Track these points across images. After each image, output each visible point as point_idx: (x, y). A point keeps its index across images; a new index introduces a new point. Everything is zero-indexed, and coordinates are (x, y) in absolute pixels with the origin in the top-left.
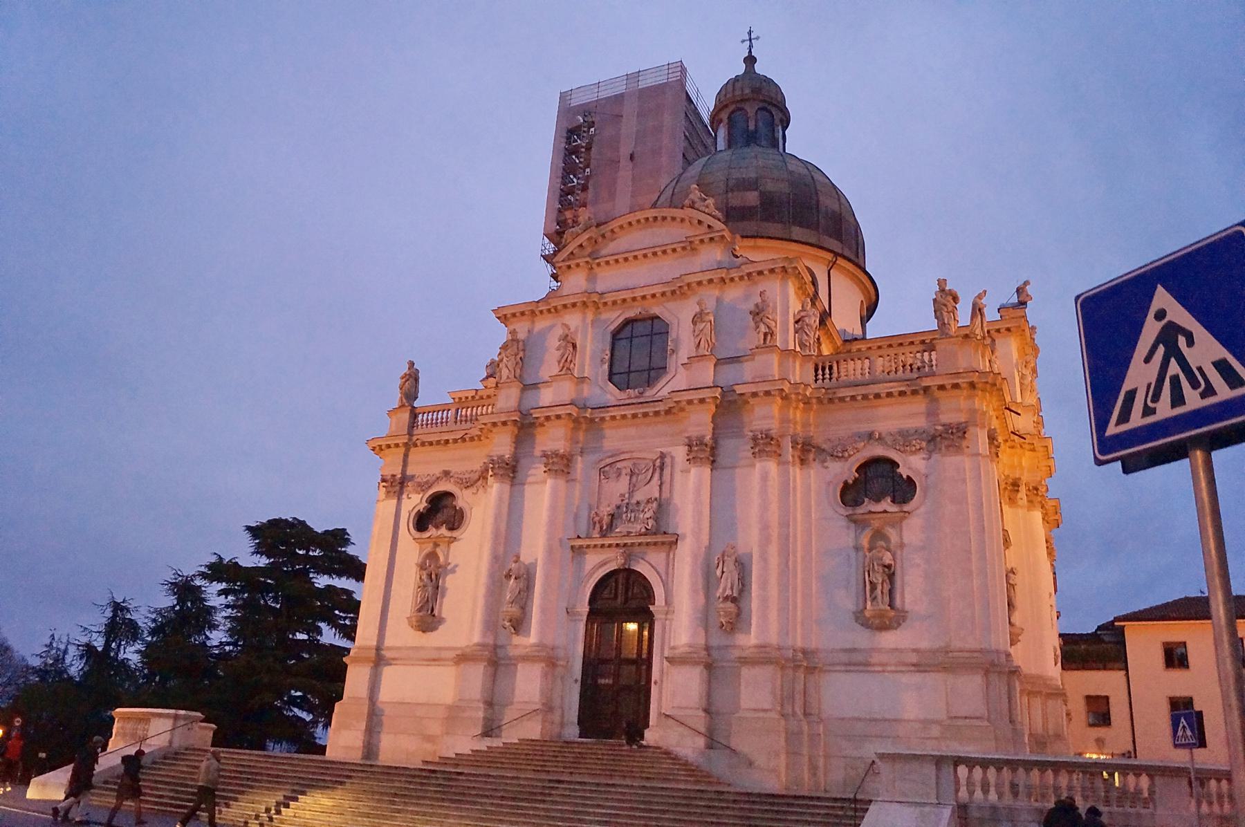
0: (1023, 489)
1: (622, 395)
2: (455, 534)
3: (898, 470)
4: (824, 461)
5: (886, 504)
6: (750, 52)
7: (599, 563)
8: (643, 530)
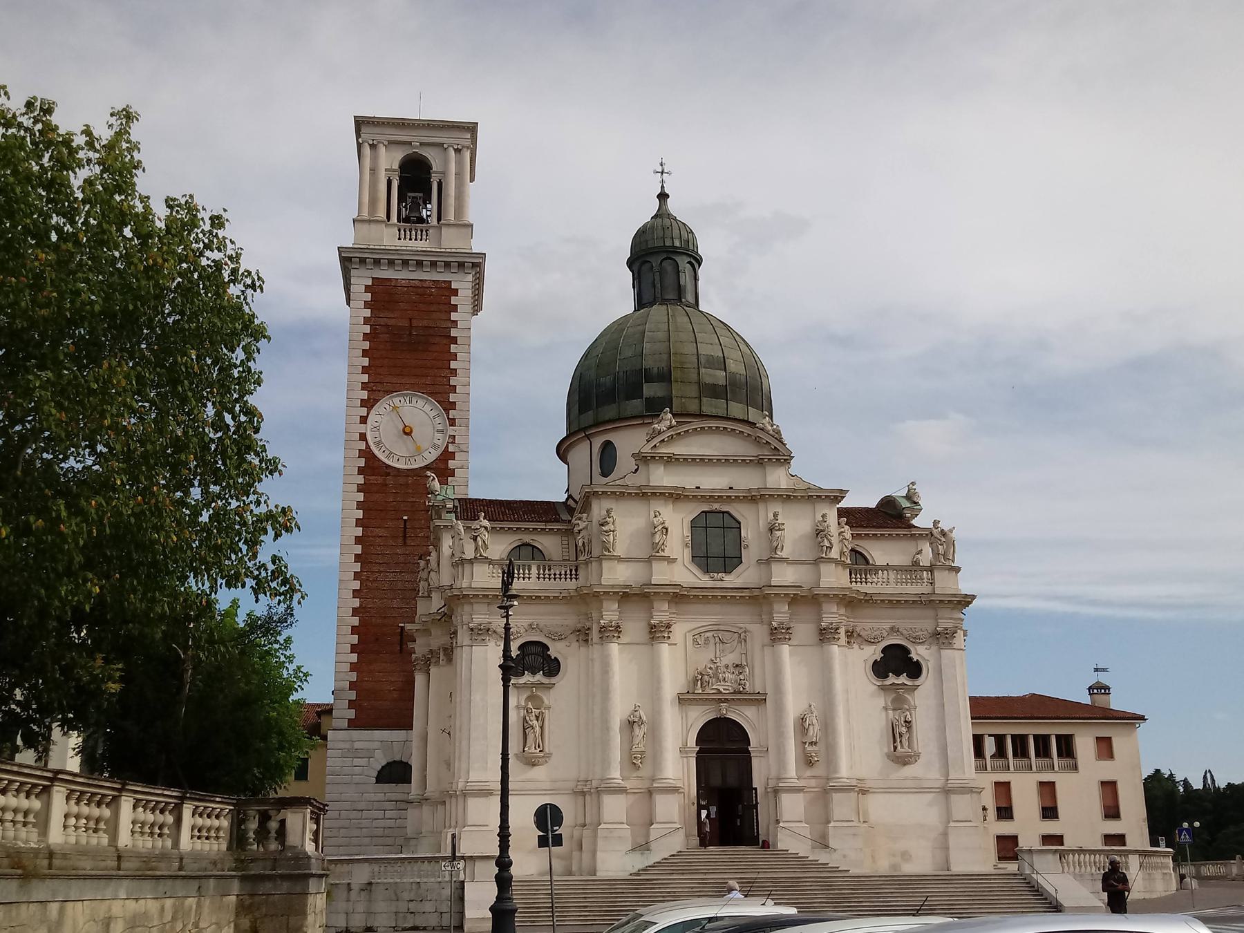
1: (706, 577)
2: (553, 680)
5: (903, 679)
6: (662, 187)
8: (741, 689)
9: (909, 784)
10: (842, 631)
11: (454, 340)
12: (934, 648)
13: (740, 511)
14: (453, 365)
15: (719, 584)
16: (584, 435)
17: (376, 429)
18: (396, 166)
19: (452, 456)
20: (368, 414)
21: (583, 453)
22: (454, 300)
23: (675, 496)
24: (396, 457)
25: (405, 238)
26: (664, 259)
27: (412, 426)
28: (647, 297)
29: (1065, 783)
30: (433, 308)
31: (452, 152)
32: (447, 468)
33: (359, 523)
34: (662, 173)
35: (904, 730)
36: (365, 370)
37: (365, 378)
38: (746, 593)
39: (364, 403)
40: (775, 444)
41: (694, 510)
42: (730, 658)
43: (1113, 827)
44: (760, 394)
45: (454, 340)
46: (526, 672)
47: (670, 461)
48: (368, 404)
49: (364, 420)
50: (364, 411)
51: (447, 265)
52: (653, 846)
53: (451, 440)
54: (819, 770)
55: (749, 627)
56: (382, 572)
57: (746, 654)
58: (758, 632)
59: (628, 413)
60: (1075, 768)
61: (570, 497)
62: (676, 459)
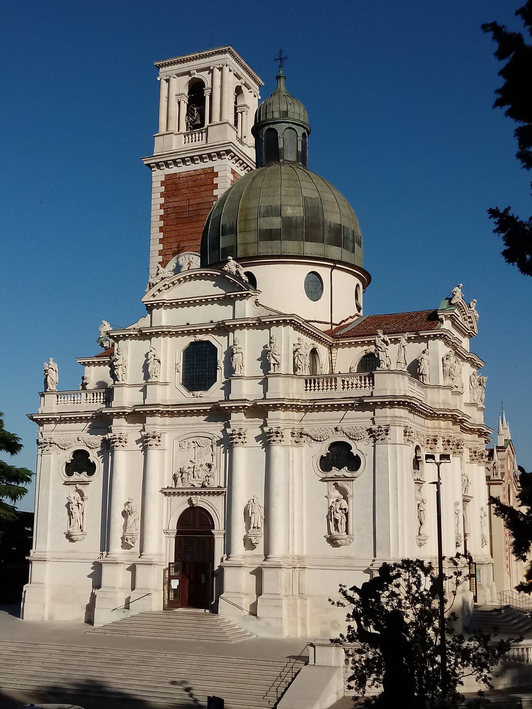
0: (440, 442)
3: (351, 451)
5: (344, 472)
9: (342, 562)
10: (287, 434)
15: (199, 400)
22: (216, 181)
25: (189, 142)
30: (202, 189)
44: (321, 229)
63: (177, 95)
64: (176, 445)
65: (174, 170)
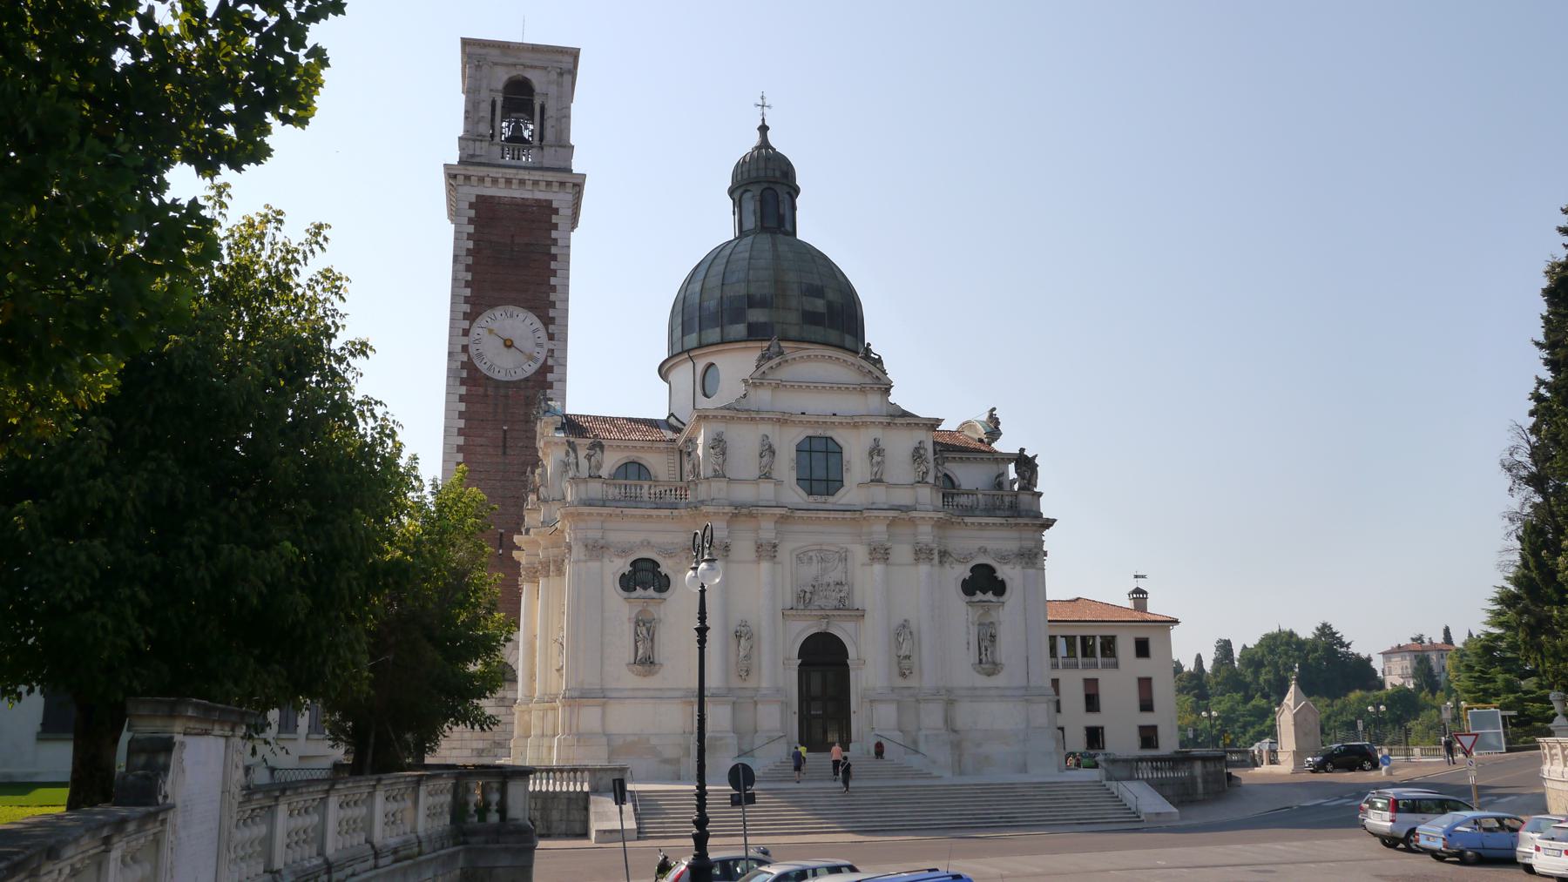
1: (811, 499)
2: (664, 595)
4: (952, 563)
5: (990, 596)
6: (763, 120)
7: (804, 628)
8: (841, 606)
11: (554, 258)
12: (1018, 568)
13: (841, 436)
14: (553, 281)
16: (687, 356)
17: (478, 341)
18: (500, 86)
19: (551, 369)
20: (470, 327)
21: (684, 374)
22: (555, 219)
23: (783, 420)
24: (497, 370)
26: (765, 189)
27: (512, 339)
28: (750, 223)
29: (1107, 679)
31: (554, 76)
32: (545, 381)
33: (461, 432)
34: (763, 106)
35: (987, 643)
36: (468, 284)
37: (468, 292)
38: (848, 515)
39: (466, 316)
40: (877, 373)
41: (796, 435)
42: (834, 575)
43: (1147, 719)
45: (554, 258)
46: (638, 588)
47: (779, 386)
48: (471, 317)
49: (466, 333)
50: (466, 324)
51: (549, 184)
52: (756, 753)
53: (550, 354)
54: (912, 682)
55: (849, 546)
56: (483, 479)
57: (846, 573)
58: (860, 552)
59: (732, 337)
60: (1116, 666)
61: (671, 415)
62: (783, 385)
63: (491, 90)
64: (794, 556)
65: (489, 191)
